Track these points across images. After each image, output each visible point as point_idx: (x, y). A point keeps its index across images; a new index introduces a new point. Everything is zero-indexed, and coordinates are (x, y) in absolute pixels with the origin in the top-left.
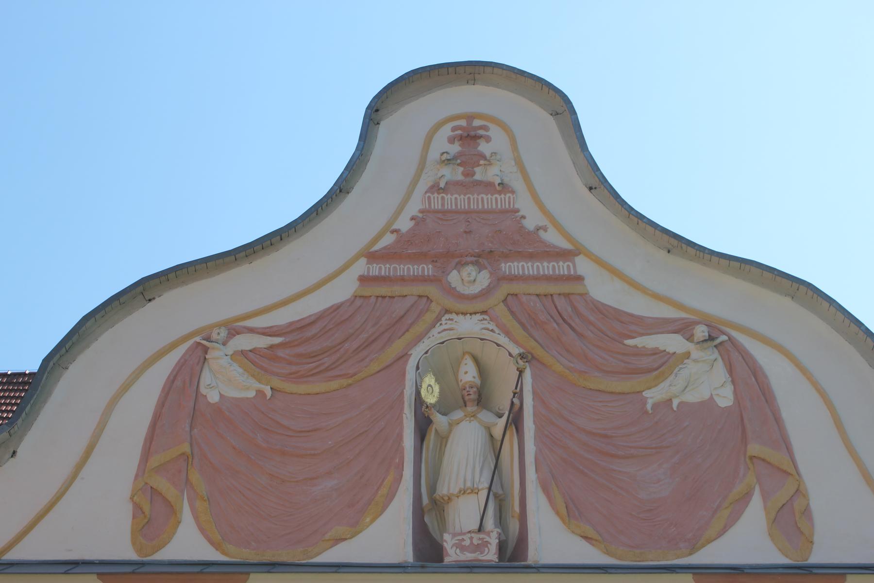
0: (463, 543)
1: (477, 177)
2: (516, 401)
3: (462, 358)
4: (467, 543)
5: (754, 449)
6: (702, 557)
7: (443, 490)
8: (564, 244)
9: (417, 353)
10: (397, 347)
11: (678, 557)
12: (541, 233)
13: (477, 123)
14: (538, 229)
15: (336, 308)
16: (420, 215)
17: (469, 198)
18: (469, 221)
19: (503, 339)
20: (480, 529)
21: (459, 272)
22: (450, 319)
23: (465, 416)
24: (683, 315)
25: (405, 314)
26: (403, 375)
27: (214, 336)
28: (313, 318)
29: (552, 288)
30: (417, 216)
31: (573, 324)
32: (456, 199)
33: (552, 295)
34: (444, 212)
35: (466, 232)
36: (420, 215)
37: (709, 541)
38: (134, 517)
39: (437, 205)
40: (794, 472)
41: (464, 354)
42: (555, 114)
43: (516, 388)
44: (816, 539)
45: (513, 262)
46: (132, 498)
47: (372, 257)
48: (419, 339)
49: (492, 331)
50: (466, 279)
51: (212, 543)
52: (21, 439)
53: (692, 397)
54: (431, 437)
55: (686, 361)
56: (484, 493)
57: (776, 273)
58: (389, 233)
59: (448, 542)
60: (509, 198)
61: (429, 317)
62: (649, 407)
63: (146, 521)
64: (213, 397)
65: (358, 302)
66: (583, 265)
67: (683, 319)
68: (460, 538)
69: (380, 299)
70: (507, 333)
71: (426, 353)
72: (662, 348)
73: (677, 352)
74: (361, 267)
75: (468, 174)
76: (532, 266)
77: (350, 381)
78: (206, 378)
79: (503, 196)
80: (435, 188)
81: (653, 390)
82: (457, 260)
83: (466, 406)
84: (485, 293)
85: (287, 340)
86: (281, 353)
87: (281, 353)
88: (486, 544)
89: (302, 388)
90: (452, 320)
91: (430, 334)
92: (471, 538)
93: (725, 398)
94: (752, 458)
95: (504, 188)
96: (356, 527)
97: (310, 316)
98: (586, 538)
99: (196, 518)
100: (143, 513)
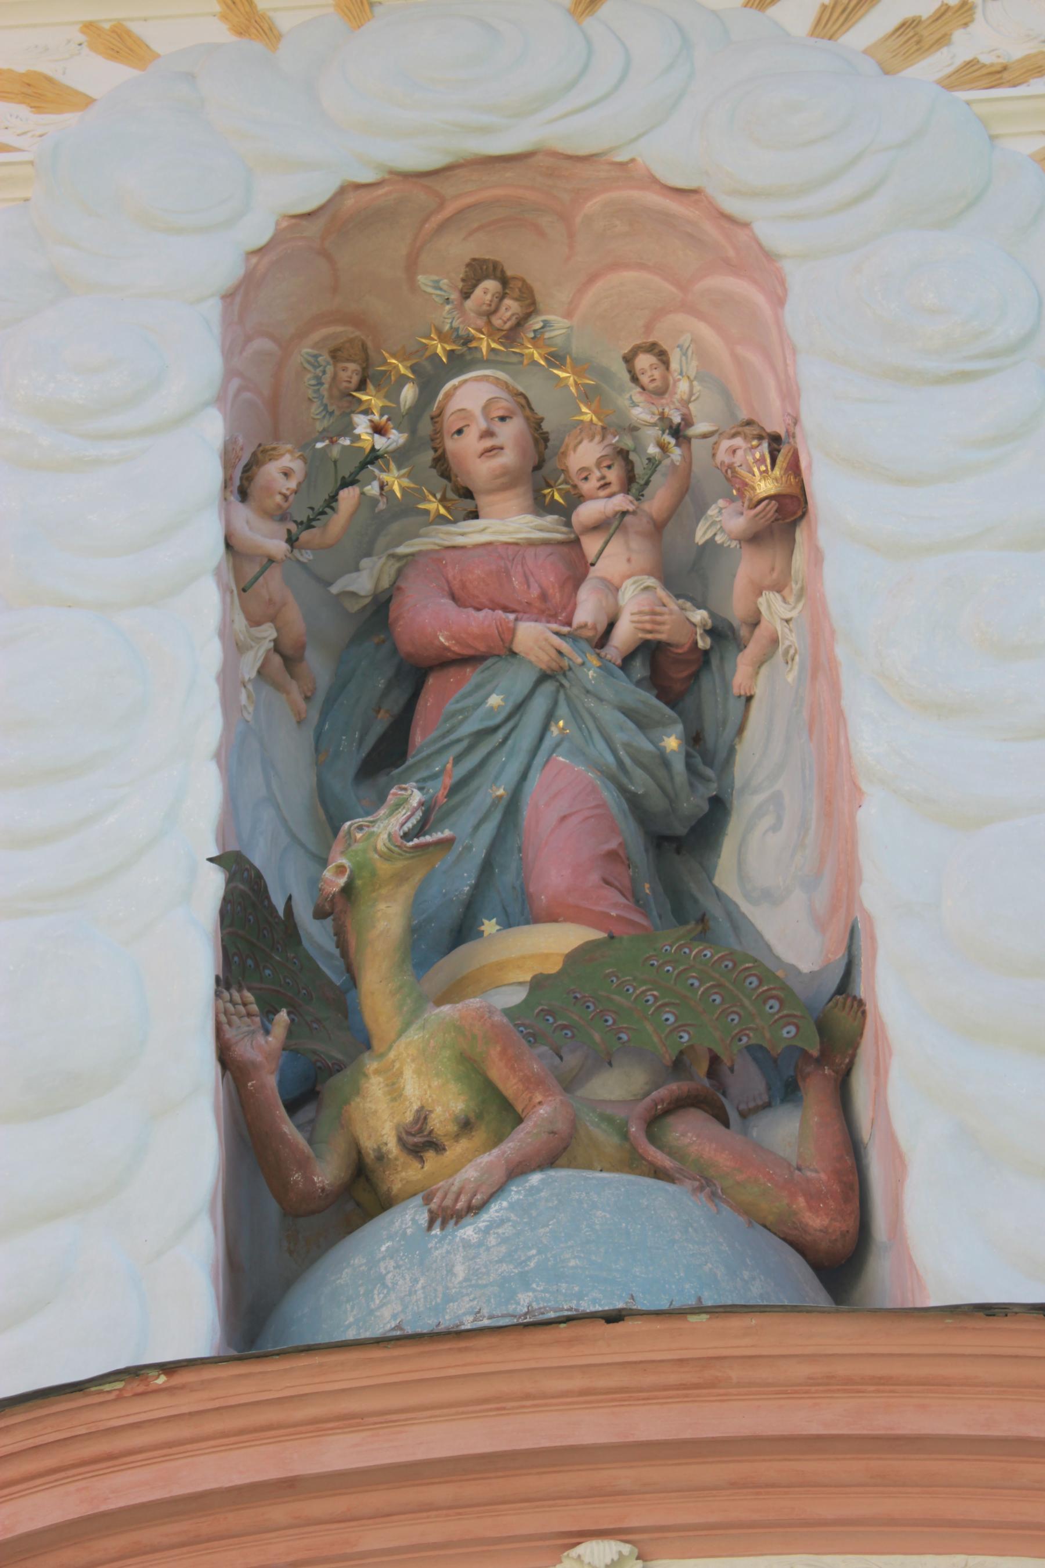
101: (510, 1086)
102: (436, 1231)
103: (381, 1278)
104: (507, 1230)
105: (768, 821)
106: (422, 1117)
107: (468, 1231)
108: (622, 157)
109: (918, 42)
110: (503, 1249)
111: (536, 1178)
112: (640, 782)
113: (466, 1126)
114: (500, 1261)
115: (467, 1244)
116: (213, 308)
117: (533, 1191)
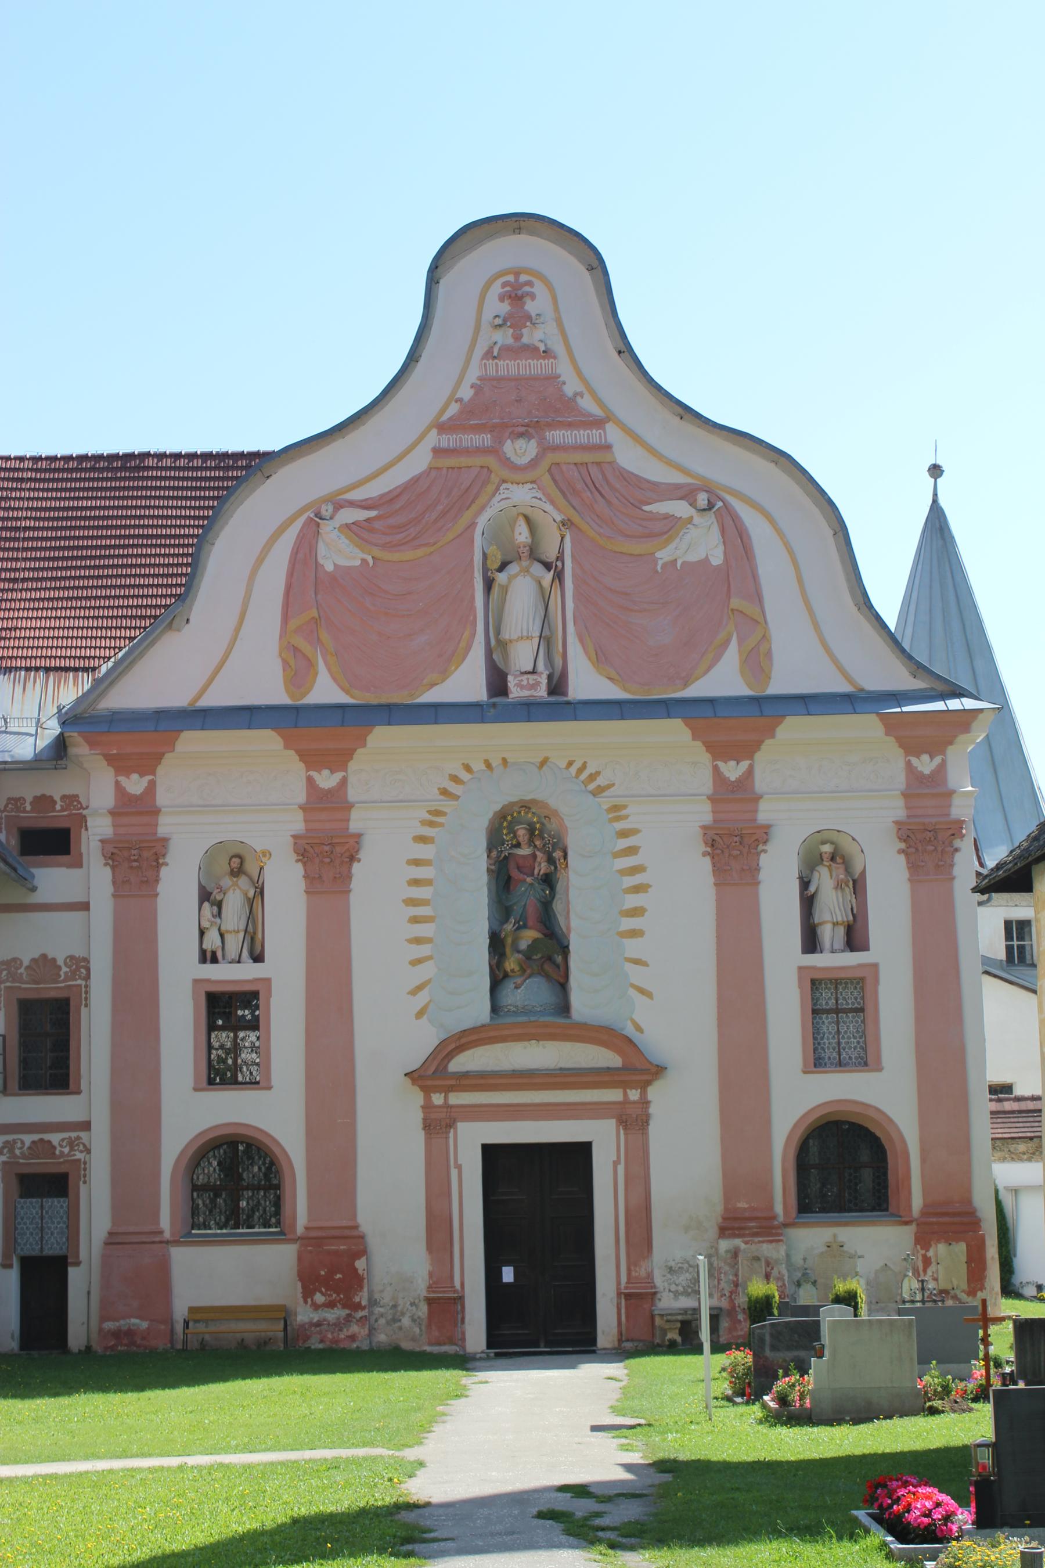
0: (522, 683)
1: (525, 340)
2: (559, 564)
3: (517, 518)
4: (525, 683)
5: (735, 603)
6: (692, 692)
7: (506, 635)
8: (596, 411)
9: (482, 521)
10: (467, 515)
11: (675, 692)
12: (579, 399)
13: (523, 278)
14: (576, 394)
15: (415, 480)
16: (478, 382)
17: (518, 364)
18: (518, 389)
19: (548, 507)
20: (534, 672)
21: (512, 442)
22: (506, 489)
23: (520, 571)
24: (689, 480)
25: (470, 485)
26: (472, 541)
27: (324, 513)
28: (399, 490)
29: (587, 457)
30: (477, 384)
31: (603, 492)
32: (508, 364)
33: (586, 463)
34: (499, 379)
35: (517, 401)
36: (478, 382)
37: (697, 679)
38: (284, 670)
39: (492, 372)
40: (763, 622)
41: (518, 515)
42: (590, 269)
43: (559, 553)
44: (773, 674)
45: (555, 431)
46: (280, 655)
47: (442, 428)
48: (483, 508)
49: (540, 499)
50: (518, 451)
51: (343, 689)
52: (191, 609)
53: (693, 557)
54: (496, 590)
55: (689, 526)
56: (537, 640)
57: (764, 445)
58: (453, 402)
59: (512, 682)
60: (552, 363)
61: (490, 488)
62: (659, 568)
63: (293, 673)
64: (329, 567)
65: (433, 473)
66: (612, 434)
67: (689, 484)
68: (520, 679)
69: (450, 470)
70: (552, 502)
71: (489, 520)
72: (671, 514)
73: (683, 517)
74: (433, 438)
75: (517, 337)
76: (571, 435)
77: (432, 549)
78: (322, 550)
79: (546, 361)
80: (489, 354)
81: (664, 551)
82: (510, 430)
83: (520, 558)
84: (534, 463)
85: (381, 513)
86: (377, 525)
87: (377, 525)
88: (538, 683)
89: (396, 556)
90: (508, 489)
91: (491, 503)
92: (528, 679)
93: (717, 559)
94: (732, 610)
95: (547, 353)
96: (444, 674)
97: (396, 488)
98: (609, 678)
99: (329, 670)
100: (290, 666)
101: (525, 967)
105: (560, 901)
106: (513, 969)
107: (519, 991)
111: (527, 981)
112: (543, 900)
113: (519, 971)
116: (484, 832)
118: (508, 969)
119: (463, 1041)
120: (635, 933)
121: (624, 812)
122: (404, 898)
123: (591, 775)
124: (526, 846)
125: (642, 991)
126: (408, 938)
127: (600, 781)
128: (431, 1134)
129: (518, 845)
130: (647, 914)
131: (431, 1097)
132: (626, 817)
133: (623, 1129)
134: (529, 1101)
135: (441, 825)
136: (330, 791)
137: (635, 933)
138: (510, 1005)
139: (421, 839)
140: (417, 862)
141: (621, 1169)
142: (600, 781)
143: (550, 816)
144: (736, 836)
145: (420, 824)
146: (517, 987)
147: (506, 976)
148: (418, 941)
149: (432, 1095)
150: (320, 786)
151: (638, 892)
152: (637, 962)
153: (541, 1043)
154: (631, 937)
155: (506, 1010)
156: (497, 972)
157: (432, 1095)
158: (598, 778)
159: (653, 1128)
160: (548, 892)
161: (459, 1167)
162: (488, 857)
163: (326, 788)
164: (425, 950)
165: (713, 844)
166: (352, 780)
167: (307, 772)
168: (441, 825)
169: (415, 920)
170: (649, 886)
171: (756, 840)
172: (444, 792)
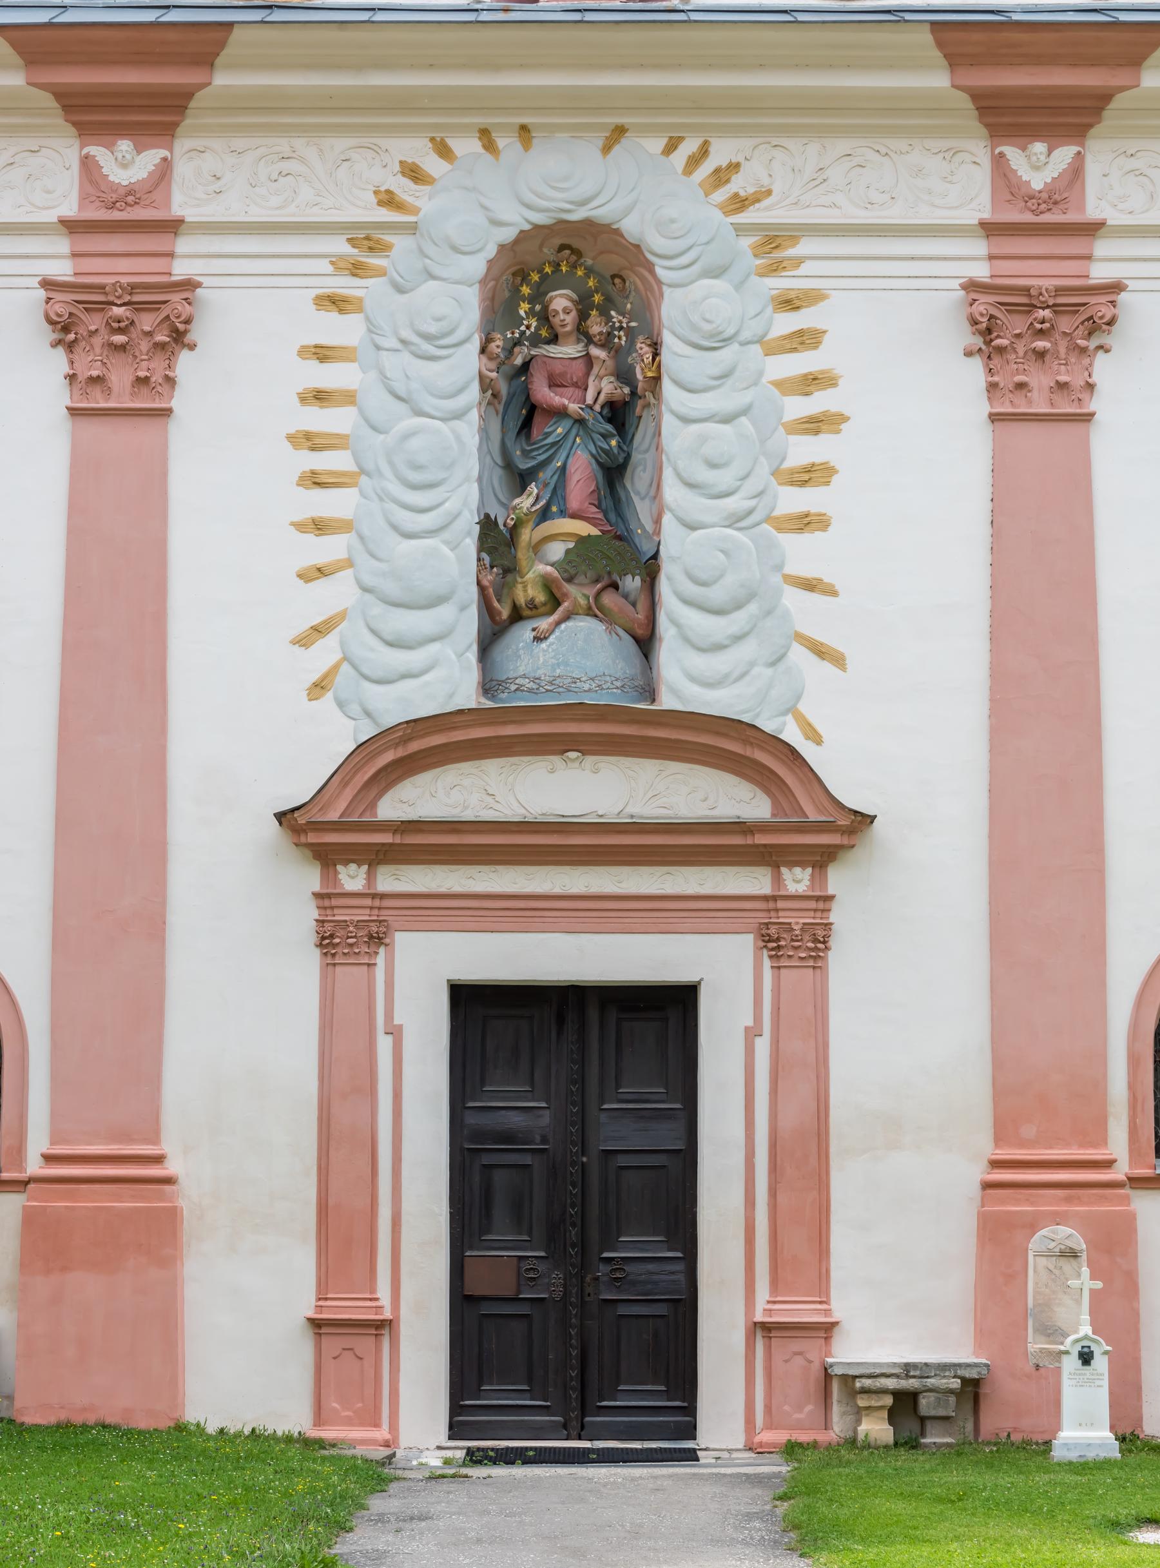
102: (535, 643)
103: (520, 656)
104: (554, 647)
106: (532, 600)
107: (544, 645)
108: (615, 227)
109: (720, 181)
110: (553, 654)
111: (563, 626)
113: (544, 604)
114: (552, 658)
115: (544, 651)
117: (562, 632)
118: (521, 600)
119: (415, 746)
120: (806, 522)
121: (791, 252)
122: (292, 431)
123: (717, 171)
124: (573, 338)
125: (820, 651)
126: (296, 519)
127: (739, 185)
128: (334, 955)
129: (554, 339)
130: (835, 479)
131: (336, 873)
132: (799, 261)
133: (771, 957)
134: (557, 890)
135: (381, 273)
136: (130, 191)
137: (806, 522)
138: (524, 676)
139: (335, 303)
140: (322, 354)
141: (763, 1045)
142: (739, 185)
143: (624, 273)
144: (1043, 309)
145: (330, 269)
146: (538, 639)
147: (517, 616)
148: (319, 526)
149: (339, 868)
150: (111, 178)
151: (817, 432)
152: (810, 585)
153: (590, 760)
154: (800, 530)
155: (513, 687)
156: (496, 604)
157: (339, 868)
158: (734, 178)
159: (836, 959)
160: (614, 443)
161: (395, 1032)
162: (483, 351)
163: (125, 183)
164: (331, 548)
165: (987, 330)
166: (183, 170)
167: (82, 148)
168: (381, 273)
169: (315, 480)
170: (842, 418)
171: (1088, 319)
172: (389, 200)
